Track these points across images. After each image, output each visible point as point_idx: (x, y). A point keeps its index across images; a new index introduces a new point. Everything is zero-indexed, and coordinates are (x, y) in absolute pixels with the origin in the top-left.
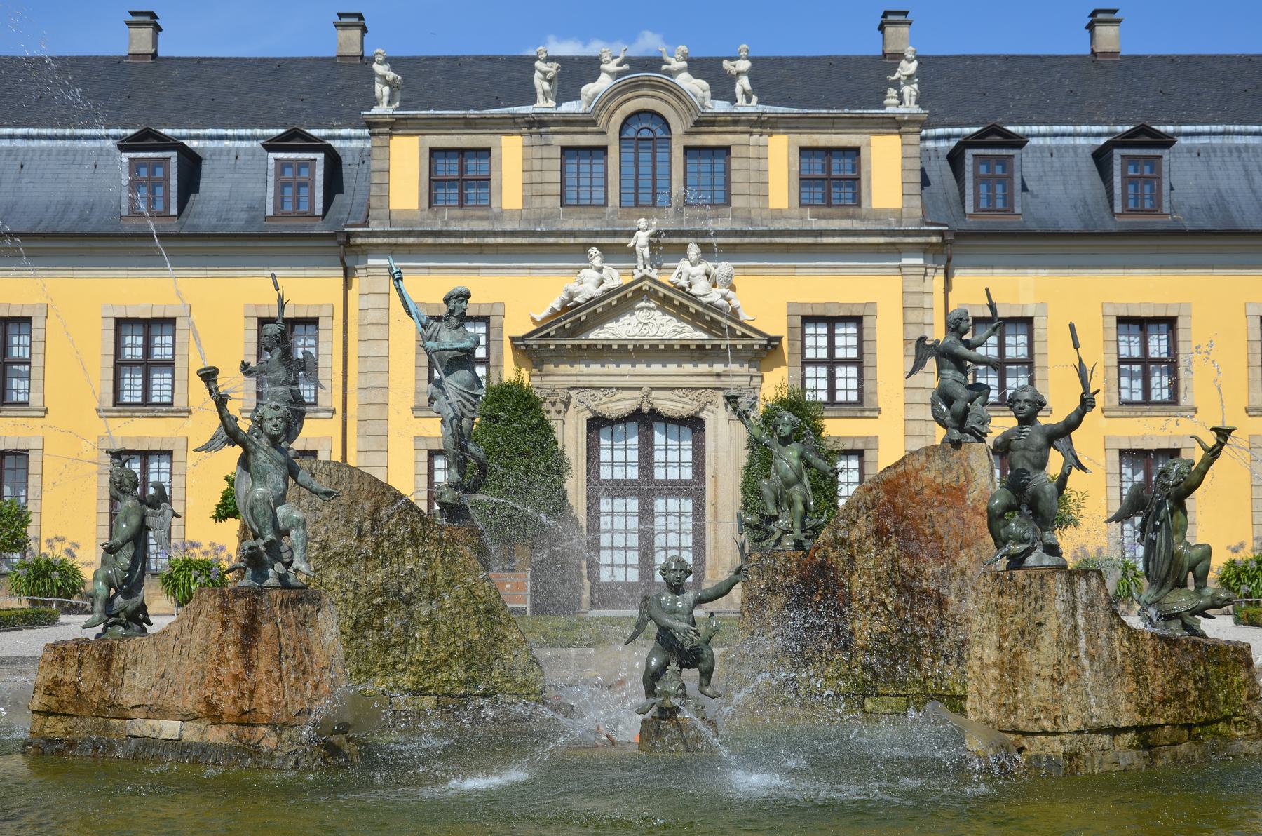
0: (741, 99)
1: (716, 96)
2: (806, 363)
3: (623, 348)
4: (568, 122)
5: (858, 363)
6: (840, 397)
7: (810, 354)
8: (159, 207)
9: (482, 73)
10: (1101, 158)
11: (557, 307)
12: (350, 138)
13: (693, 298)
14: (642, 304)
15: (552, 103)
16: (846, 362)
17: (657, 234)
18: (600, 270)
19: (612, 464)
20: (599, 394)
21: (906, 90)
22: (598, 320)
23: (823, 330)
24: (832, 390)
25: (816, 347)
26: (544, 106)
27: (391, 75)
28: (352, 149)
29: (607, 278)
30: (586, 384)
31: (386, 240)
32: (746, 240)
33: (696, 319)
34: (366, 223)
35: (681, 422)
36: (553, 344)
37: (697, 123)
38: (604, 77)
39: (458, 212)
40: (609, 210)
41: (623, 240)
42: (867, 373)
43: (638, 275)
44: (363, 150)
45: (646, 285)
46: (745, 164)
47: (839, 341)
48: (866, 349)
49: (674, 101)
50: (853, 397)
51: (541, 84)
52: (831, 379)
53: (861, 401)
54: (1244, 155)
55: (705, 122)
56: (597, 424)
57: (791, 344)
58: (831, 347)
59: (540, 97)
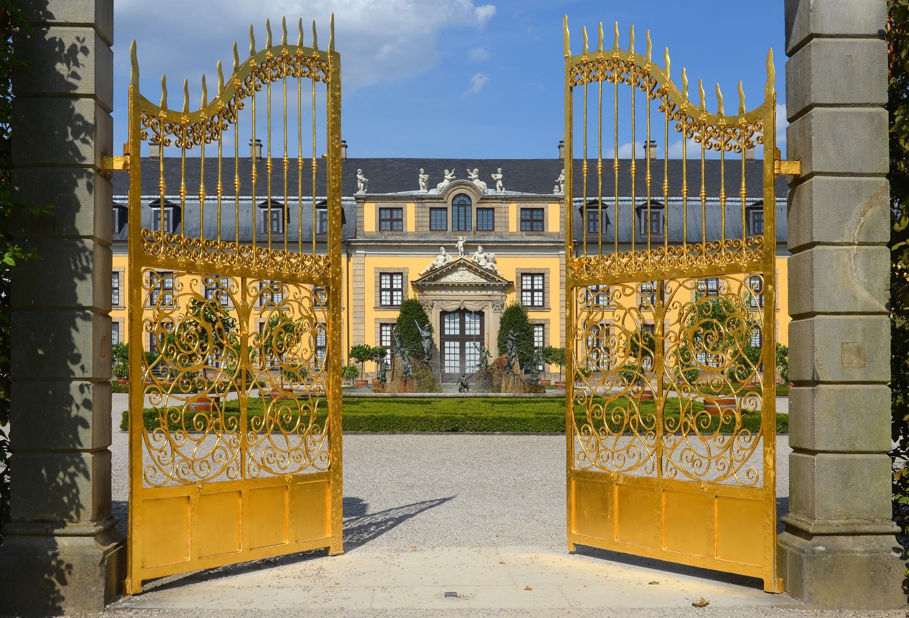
0: (499, 190)
1: (489, 187)
2: (523, 291)
3: (453, 285)
4: (432, 198)
5: (542, 291)
6: (536, 304)
7: (524, 287)
8: (275, 229)
9: (396, 167)
10: (638, 210)
11: (428, 270)
12: (346, 200)
13: (480, 267)
14: (461, 268)
15: (426, 191)
16: (538, 291)
17: (467, 242)
18: (445, 256)
19: (450, 329)
20: (444, 302)
21: (562, 186)
22: (444, 275)
23: (529, 278)
24: (533, 301)
25: (527, 285)
26: (422, 192)
27: (364, 179)
28: (347, 205)
29: (447, 259)
30: (440, 299)
31: (363, 244)
32: (500, 244)
33: (481, 274)
34: (355, 237)
35: (476, 313)
36: (427, 284)
37: (482, 199)
38: (446, 181)
39: (390, 233)
40: (448, 232)
41: (454, 244)
42: (546, 295)
43: (459, 258)
44: (352, 205)
45: (462, 262)
46: (500, 215)
47: (536, 282)
48: (546, 285)
49: (473, 190)
50: (541, 304)
51: (422, 183)
52: (532, 297)
53: (543, 306)
54: (695, 209)
55: (485, 199)
56: (444, 314)
57: (517, 284)
58: (533, 285)
59: (421, 188)
